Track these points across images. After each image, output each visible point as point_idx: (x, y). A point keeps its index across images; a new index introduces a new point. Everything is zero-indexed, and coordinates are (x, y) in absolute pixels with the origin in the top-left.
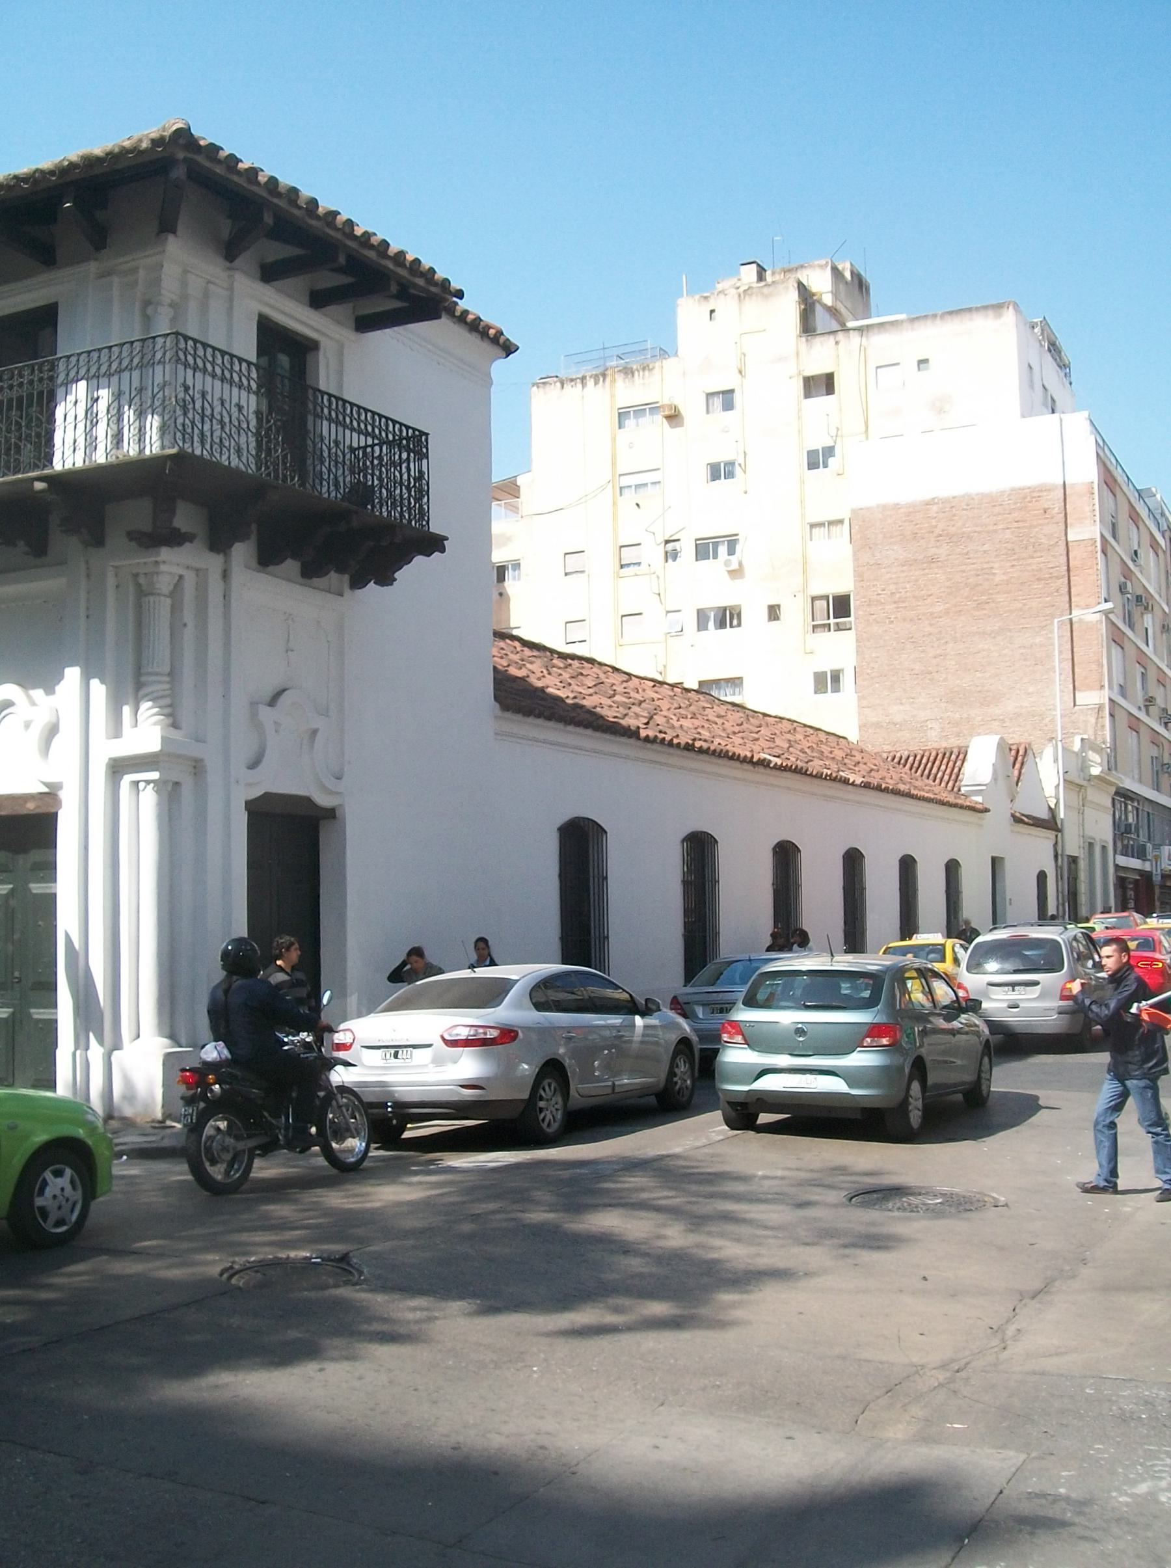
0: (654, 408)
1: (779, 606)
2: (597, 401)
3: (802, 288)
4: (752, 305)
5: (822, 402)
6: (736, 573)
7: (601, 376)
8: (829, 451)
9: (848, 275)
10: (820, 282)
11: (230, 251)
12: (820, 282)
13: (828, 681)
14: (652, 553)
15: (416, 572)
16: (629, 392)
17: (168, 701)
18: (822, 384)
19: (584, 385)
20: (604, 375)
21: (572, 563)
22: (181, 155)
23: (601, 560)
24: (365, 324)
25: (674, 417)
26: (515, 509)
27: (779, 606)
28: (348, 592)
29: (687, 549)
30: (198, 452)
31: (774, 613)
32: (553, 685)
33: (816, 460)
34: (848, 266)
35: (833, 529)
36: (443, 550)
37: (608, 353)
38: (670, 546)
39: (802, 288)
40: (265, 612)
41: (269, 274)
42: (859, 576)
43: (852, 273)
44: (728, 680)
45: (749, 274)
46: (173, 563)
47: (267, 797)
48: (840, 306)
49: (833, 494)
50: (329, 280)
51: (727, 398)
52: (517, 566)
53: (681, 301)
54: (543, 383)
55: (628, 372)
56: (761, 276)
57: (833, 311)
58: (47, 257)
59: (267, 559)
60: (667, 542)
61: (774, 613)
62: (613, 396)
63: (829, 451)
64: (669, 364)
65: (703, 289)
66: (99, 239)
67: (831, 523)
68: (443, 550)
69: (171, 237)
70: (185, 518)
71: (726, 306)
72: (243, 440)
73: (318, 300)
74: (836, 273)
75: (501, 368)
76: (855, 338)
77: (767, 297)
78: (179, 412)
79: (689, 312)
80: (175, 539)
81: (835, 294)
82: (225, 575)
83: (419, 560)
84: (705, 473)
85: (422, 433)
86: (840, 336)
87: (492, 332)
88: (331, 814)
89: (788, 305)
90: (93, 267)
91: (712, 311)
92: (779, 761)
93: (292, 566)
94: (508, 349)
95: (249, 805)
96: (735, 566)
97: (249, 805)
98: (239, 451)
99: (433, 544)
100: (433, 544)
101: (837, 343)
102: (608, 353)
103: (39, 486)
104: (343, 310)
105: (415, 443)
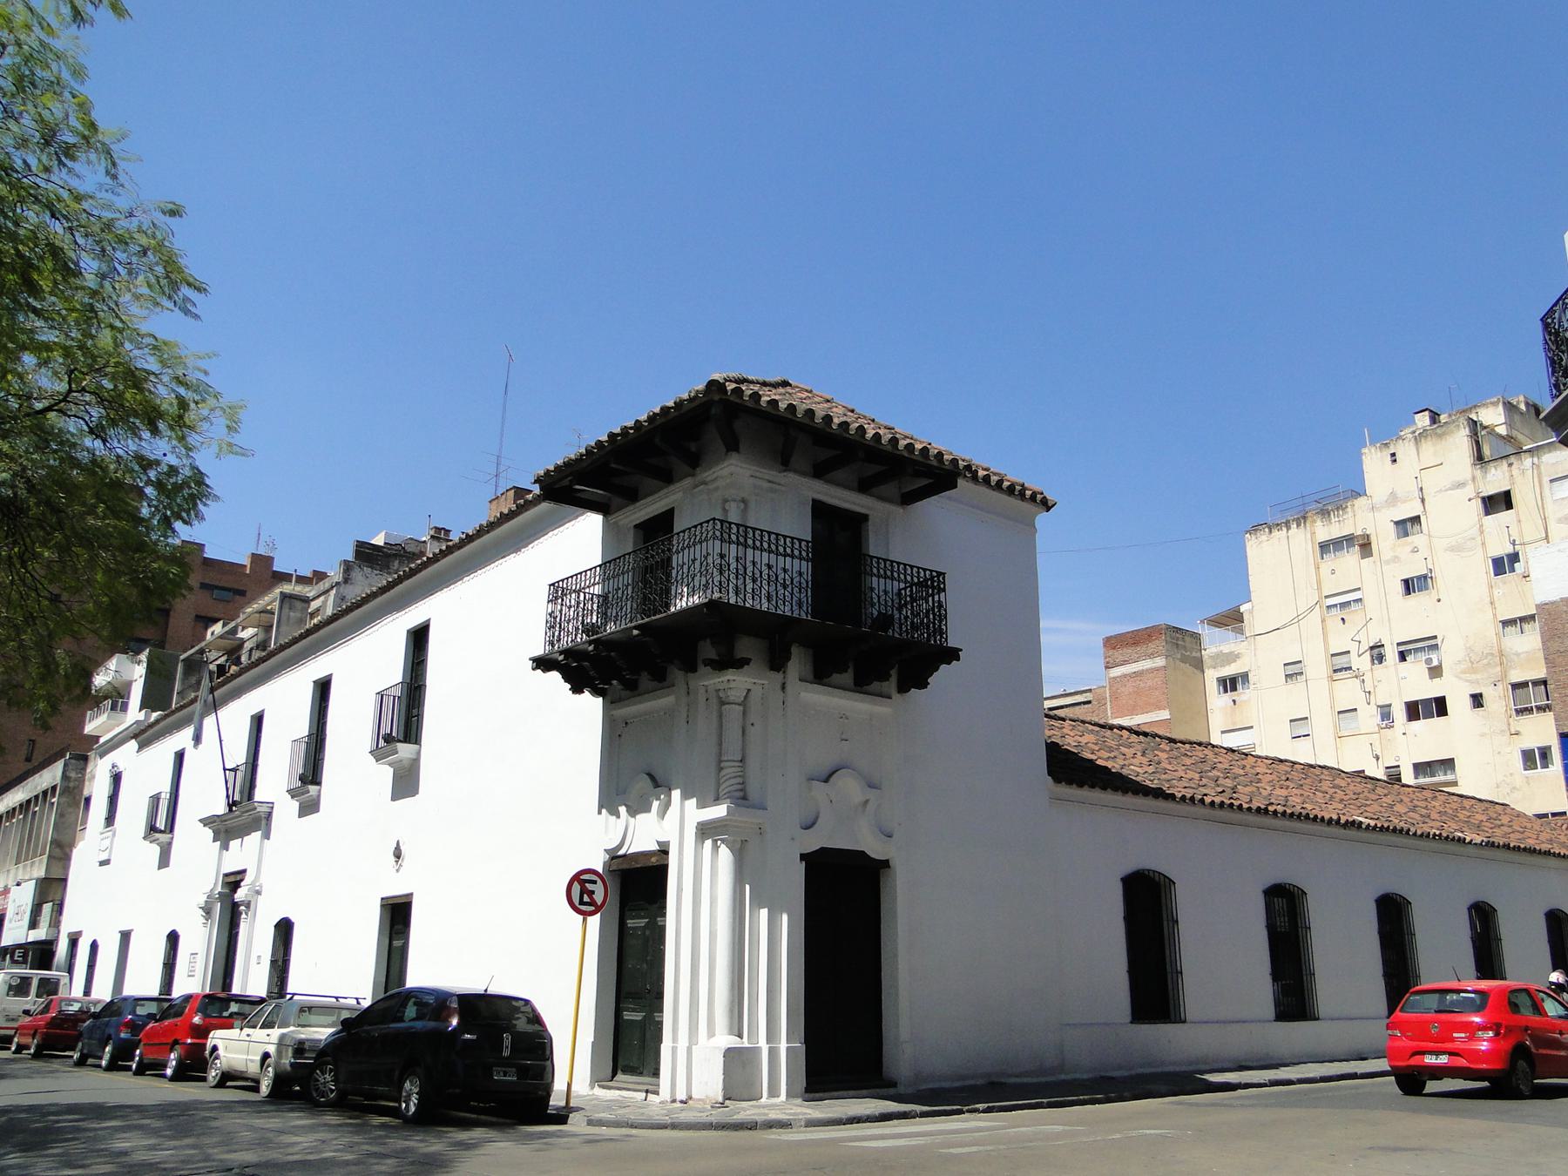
0: (1349, 540)
1: (1481, 695)
2: (1299, 542)
3: (1474, 425)
4: (1428, 447)
5: (1504, 516)
6: (1435, 672)
7: (1302, 519)
8: (1514, 557)
9: (1523, 407)
10: (1493, 416)
11: (784, 461)
12: (1493, 416)
13: (1534, 758)
14: (1362, 663)
15: (943, 676)
16: (1326, 530)
17: (740, 780)
18: (1499, 502)
19: (1288, 528)
20: (1305, 518)
21: (1294, 672)
22: (717, 398)
23: (1317, 668)
24: (908, 499)
25: (1366, 547)
26: (1241, 631)
27: (1481, 695)
28: (896, 696)
29: (1391, 653)
30: (732, 601)
31: (1477, 700)
32: (1136, 767)
33: (1504, 565)
34: (1522, 398)
35: (1526, 626)
36: (958, 659)
37: (1307, 500)
38: (1376, 651)
39: (1474, 425)
40: (813, 715)
41: (820, 471)
42: (1549, 662)
43: (1527, 404)
44: (1443, 762)
45: (1423, 420)
46: (736, 682)
47: (822, 849)
48: (1515, 433)
49: (1516, 597)
50: (873, 469)
51: (1407, 526)
52: (1245, 677)
53: (1365, 450)
54: (1255, 529)
55: (1325, 513)
56: (1434, 418)
57: (1508, 439)
58: (667, 478)
59: (820, 675)
60: (1372, 648)
61: (1477, 700)
62: (1313, 533)
63: (1514, 557)
64: (1360, 502)
65: (1386, 437)
66: (694, 462)
67: (1523, 619)
68: (958, 659)
69: (734, 454)
70: (746, 646)
71: (1405, 450)
72: (772, 588)
73: (864, 487)
74: (1510, 408)
75: (1042, 519)
76: (1528, 461)
77: (1440, 436)
78: (716, 573)
79: (1373, 462)
80: (740, 664)
81: (1509, 423)
82: (783, 687)
83: (943, 667)
84: (1400, 588)
85: (940, 574)
86: (1512, 459)
87: (1028, 493)
88: (885, 864)
89: (1460, 441)
90: (688, 482)
91: (1393, 455)
92: (1372, 823)
93: (847, 678)
94: (1046, 505)
95: (803, 857)
96: (1435, 663)
97: (803, 857)
98: (769, 598)
99: (952, 655)
100: (952, 655)
101: (1510, 465)
102: (1307, 500)
103: (635, 632)
104: (891, 488)
105: (933, 583)
